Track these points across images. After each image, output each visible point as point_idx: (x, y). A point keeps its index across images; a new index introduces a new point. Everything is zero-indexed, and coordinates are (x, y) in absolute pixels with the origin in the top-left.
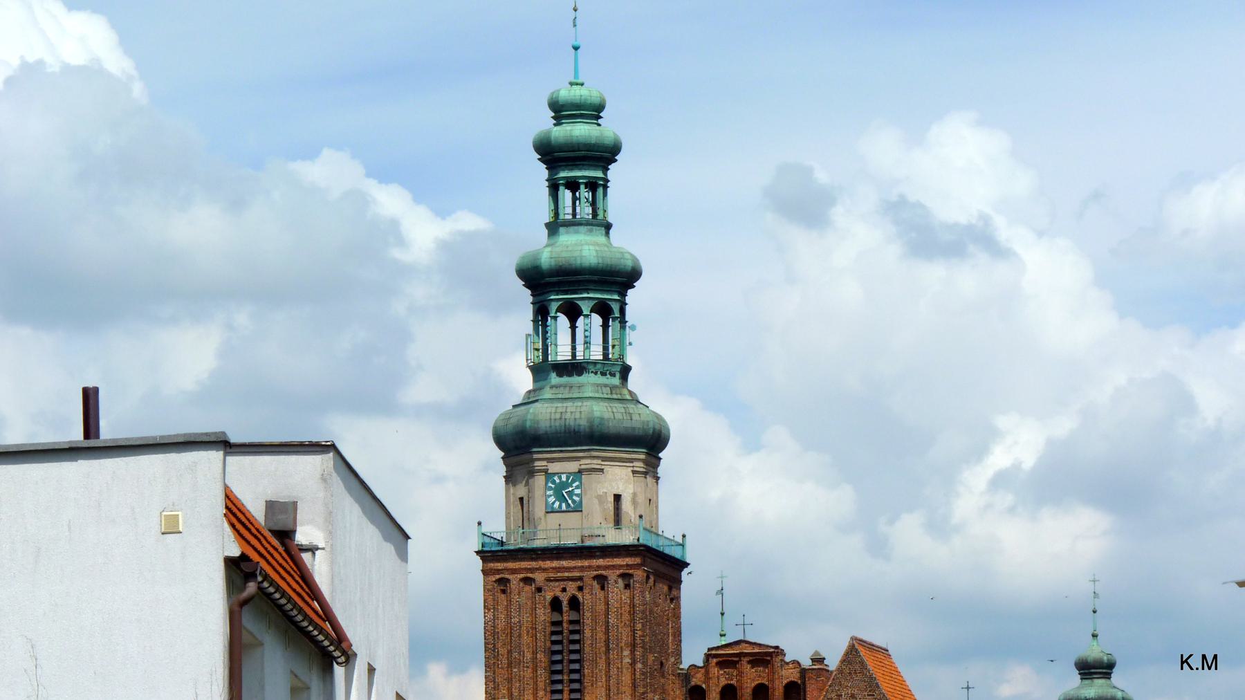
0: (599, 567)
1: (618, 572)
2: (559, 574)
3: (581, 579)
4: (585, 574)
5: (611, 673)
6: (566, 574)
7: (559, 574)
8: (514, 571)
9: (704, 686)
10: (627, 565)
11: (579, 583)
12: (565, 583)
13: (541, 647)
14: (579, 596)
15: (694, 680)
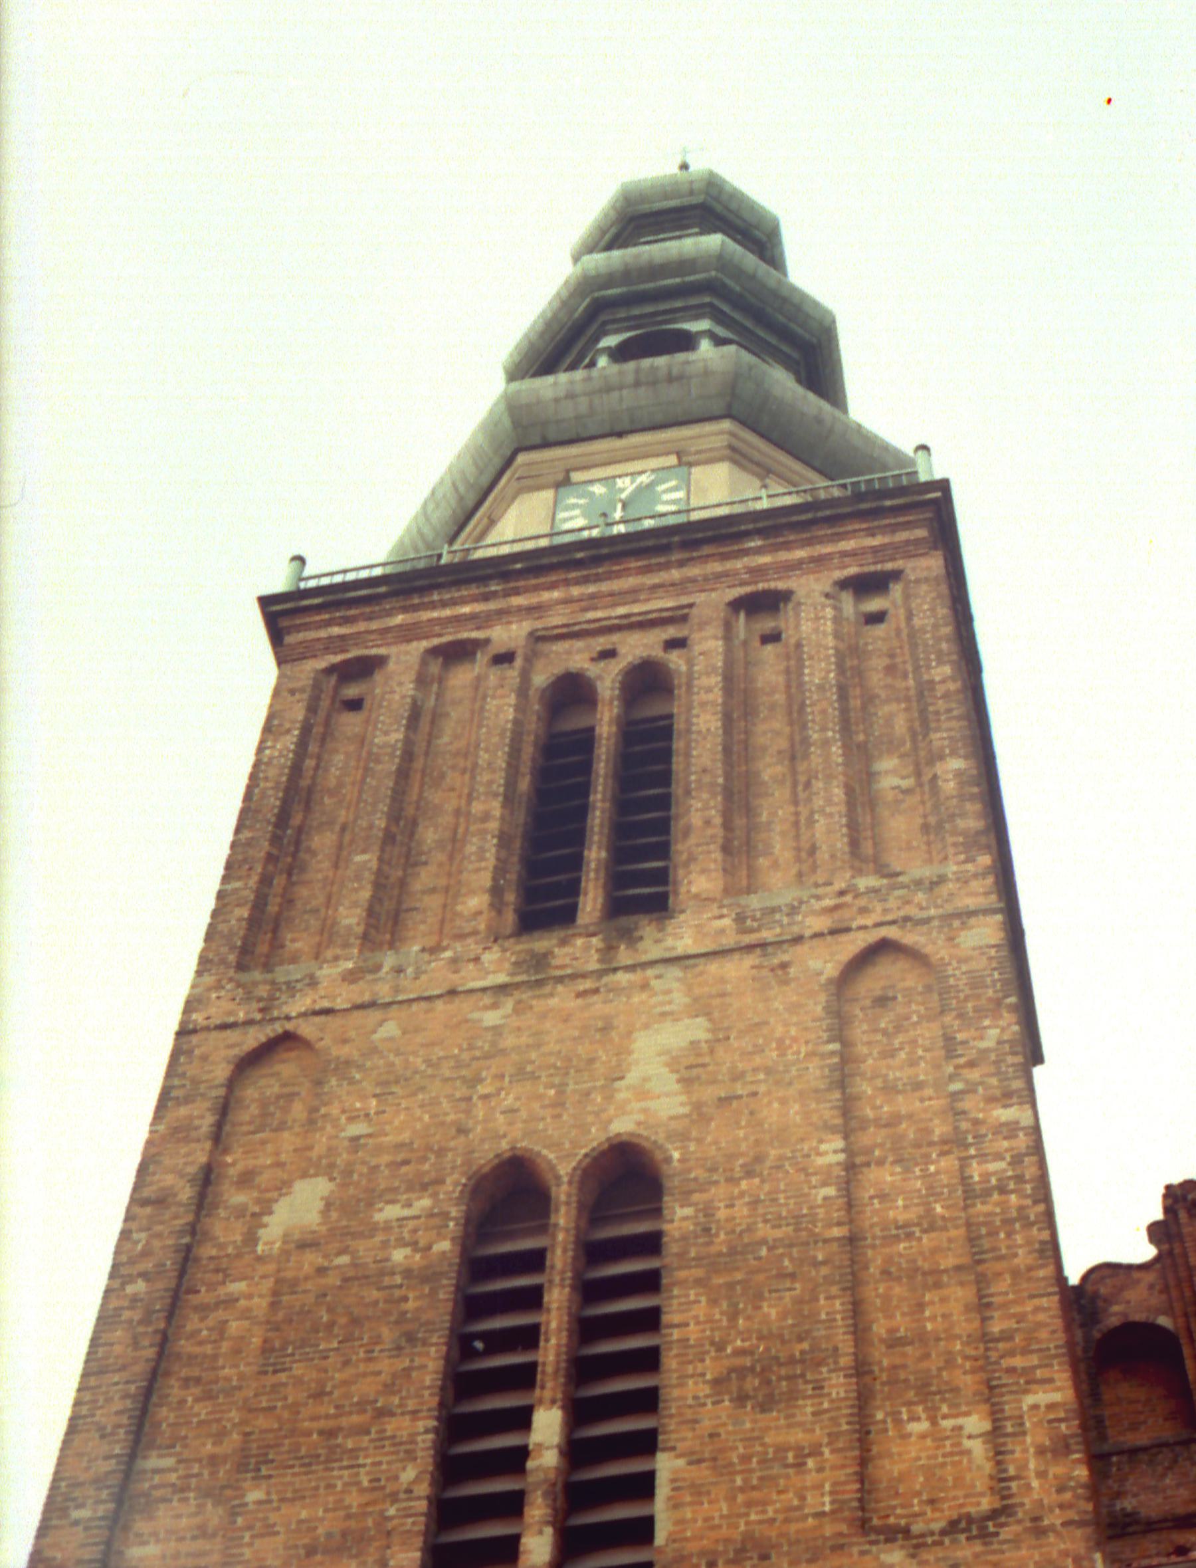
0: (758, 572)
1: (838, 574)
2: (591, 615)
3: (679, 617)
4: (700, 598)
5: (818, 802)
6: (621, 611)
7: (591, 615)
8: (408, 634)
9: (1163, 1321)
10: (875, 550)
11: (671, 632)
12: (615, 638)
13: (490, 782)
14: (676, 660)
15: (1116, 1308)
